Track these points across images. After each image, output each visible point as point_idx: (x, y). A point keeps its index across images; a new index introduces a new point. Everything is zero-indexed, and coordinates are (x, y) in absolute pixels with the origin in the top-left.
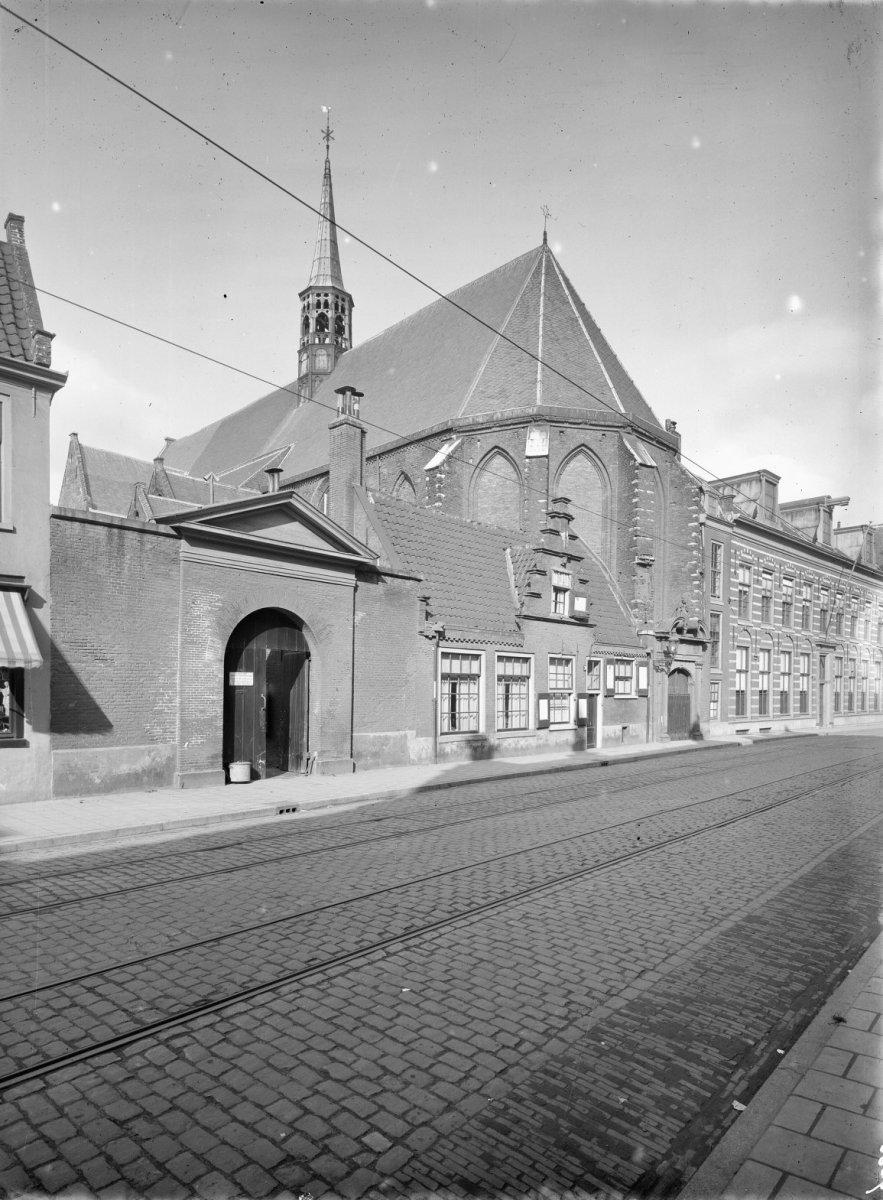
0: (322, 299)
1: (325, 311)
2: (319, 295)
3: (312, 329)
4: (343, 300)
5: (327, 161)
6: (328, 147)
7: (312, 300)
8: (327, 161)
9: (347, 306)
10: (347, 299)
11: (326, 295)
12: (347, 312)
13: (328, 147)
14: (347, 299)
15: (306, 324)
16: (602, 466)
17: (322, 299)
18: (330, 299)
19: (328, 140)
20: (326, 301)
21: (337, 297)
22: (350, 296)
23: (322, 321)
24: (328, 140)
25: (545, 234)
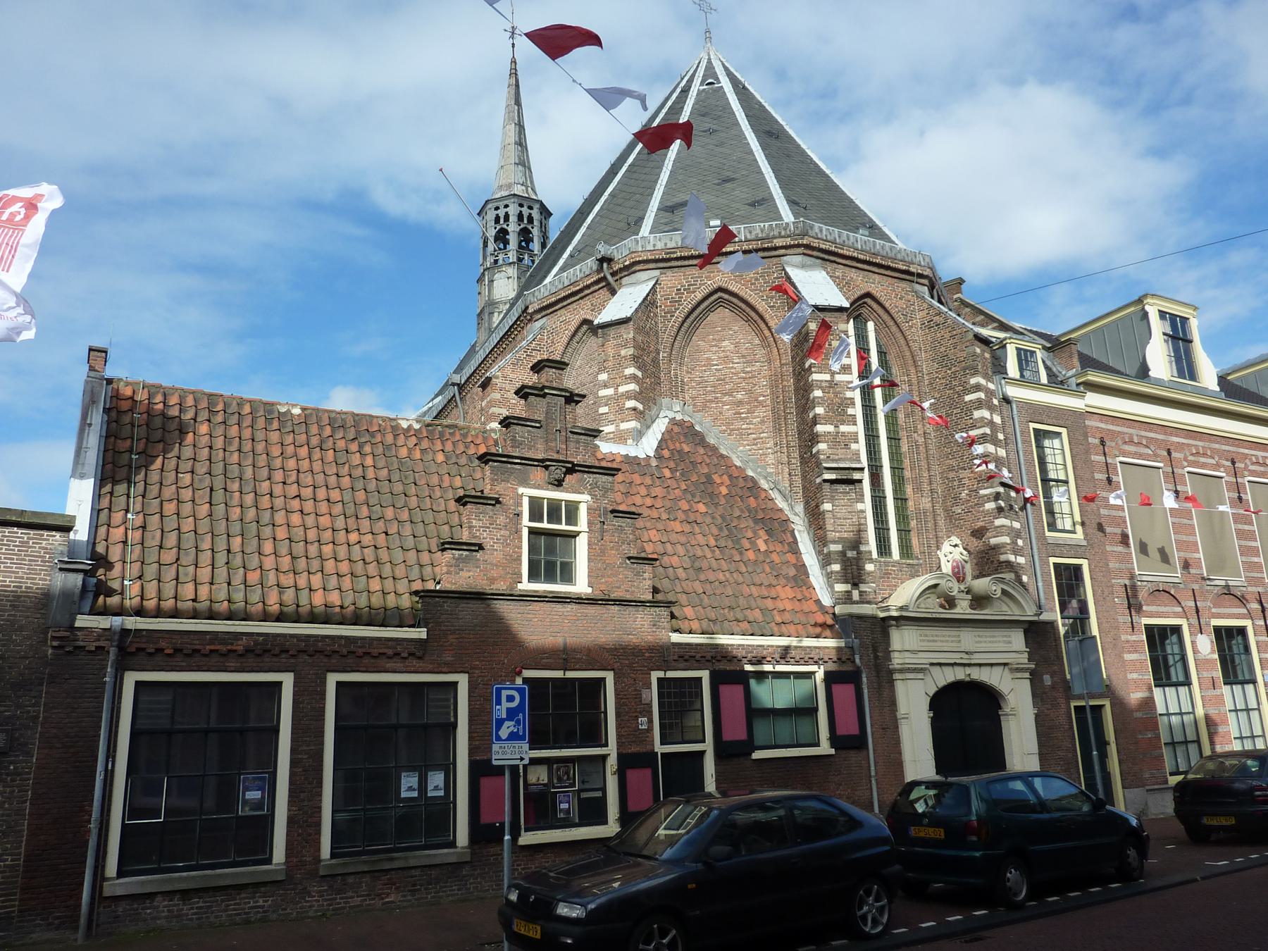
0: (501, 213)
1: (505, 226)
2: (497, 208)
4: (530, 208)
5: (514, 62)
6: (513, 45)
7: (491, 215)
8: (514, 62)
11: (506, 206)
12: (536, 223)
13: (513, 45)
14: (536, 206)
15: (485, 245)
16: (756, 317)
18: (513, 210)
20: (507, 213)
21: (521, 205)
23: (502, 236)
25: (708, 31)
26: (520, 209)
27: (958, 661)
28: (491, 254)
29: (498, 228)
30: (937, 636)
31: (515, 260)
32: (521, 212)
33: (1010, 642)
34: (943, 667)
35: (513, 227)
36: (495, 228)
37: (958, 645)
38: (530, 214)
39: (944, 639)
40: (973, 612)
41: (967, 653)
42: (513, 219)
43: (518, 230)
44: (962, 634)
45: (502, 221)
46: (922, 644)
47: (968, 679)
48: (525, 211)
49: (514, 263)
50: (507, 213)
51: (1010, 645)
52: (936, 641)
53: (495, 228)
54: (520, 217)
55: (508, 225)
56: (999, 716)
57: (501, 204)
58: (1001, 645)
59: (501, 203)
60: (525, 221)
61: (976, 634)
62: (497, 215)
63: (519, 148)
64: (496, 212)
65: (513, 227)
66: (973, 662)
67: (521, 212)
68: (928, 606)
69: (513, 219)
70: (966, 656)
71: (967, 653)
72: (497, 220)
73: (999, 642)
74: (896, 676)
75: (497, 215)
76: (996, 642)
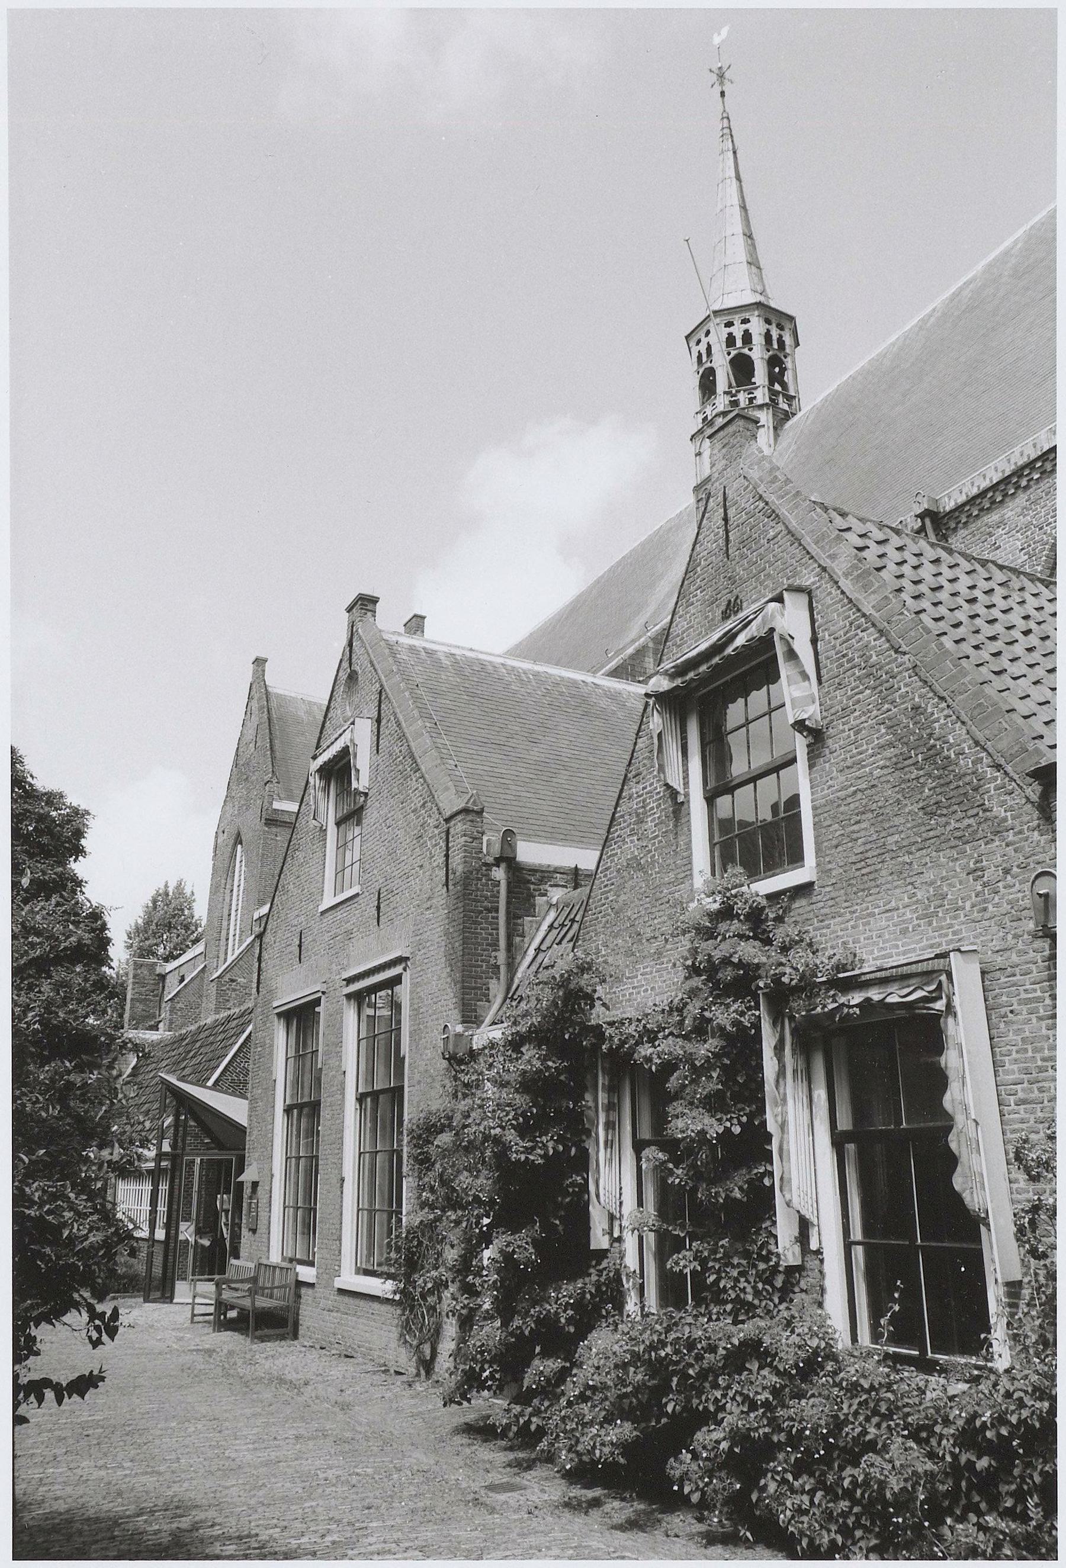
0: (738, 331)
1: (746, 351)
2: (729, 324)
3: (721, 384)
4: (780, 327)
7: (718, 336)
9: (788, 339)
10: (788, 325)
11: (745, 321)
17: (738, 331)
18: (757, 327)
19: (722, 84)
20: (746, 332)
21: (768, 321)
22: (791, 319)
23: (742, 368)
24: (722, 84)
26: (767, 326)
28: (725, 393)
29: (733, 353)
31: (767, 400)
32: (768, 331)
35: (758, 354)
36: (729, 354)
38: (781, 336)
42: (758, 340)
43: (766, 357)
45: (739, 343)
48: (775, 333)
49: (767, 404)
50: (746, 332)
53: (729, 354)
54: (768, 337)
55: (750, 349)
57: (737, 319)
59: (737, 317)
60: (776, 346)
62: (730, 334)
63: (749, 242)
64: (728, 330)
65: (758, 354)
67: (768, 331)
69: (758, 340)
72: (731, 341)
75: (730, 334)
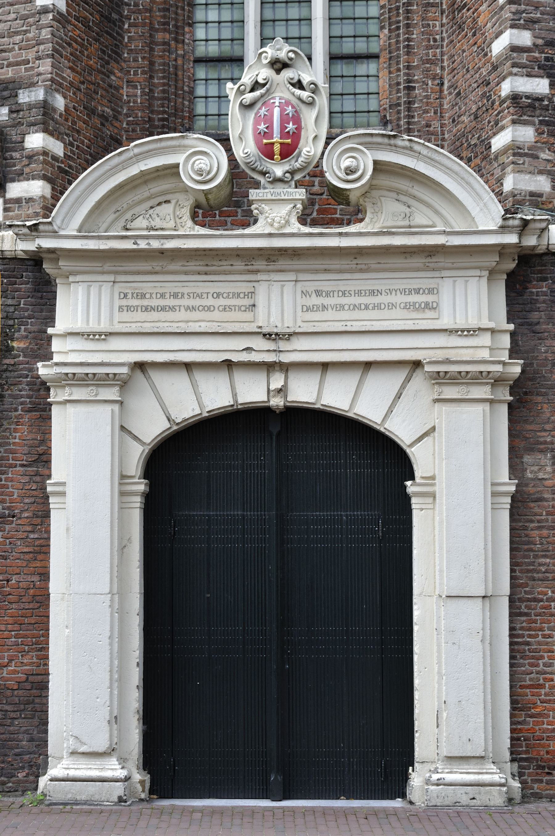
27: (235, 358)
30: (175, 296)
33: (428, 306)
34: (200, 377)
37: (248, 316)
39: (197, 302)
40: (307, 230)
41: (267, 336)
44: (262, 290)
46: (127, 316)
47: (277, 402)
51: (429, 314)
52: (172, 309)
56: (407, 499)
58: (397, 313)
61: (311, 287)
66: (286, 358)
68: (157, 223)
70: (271, 345)
71: (267, 336)
73: (392, 306)
74: (55, 396)
76: (378, 307)
